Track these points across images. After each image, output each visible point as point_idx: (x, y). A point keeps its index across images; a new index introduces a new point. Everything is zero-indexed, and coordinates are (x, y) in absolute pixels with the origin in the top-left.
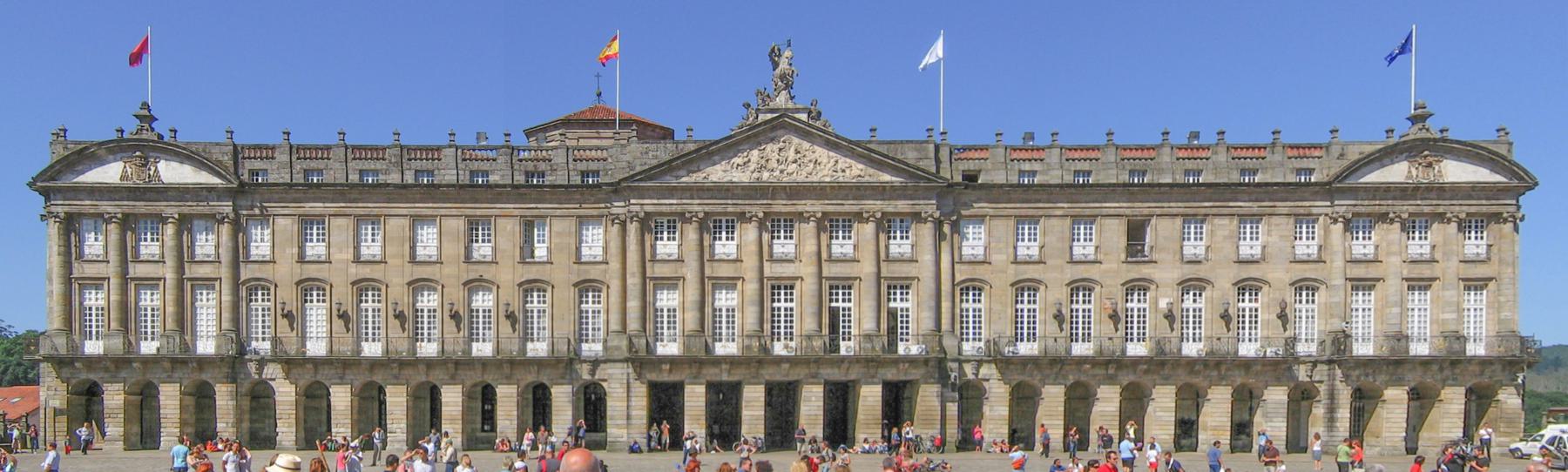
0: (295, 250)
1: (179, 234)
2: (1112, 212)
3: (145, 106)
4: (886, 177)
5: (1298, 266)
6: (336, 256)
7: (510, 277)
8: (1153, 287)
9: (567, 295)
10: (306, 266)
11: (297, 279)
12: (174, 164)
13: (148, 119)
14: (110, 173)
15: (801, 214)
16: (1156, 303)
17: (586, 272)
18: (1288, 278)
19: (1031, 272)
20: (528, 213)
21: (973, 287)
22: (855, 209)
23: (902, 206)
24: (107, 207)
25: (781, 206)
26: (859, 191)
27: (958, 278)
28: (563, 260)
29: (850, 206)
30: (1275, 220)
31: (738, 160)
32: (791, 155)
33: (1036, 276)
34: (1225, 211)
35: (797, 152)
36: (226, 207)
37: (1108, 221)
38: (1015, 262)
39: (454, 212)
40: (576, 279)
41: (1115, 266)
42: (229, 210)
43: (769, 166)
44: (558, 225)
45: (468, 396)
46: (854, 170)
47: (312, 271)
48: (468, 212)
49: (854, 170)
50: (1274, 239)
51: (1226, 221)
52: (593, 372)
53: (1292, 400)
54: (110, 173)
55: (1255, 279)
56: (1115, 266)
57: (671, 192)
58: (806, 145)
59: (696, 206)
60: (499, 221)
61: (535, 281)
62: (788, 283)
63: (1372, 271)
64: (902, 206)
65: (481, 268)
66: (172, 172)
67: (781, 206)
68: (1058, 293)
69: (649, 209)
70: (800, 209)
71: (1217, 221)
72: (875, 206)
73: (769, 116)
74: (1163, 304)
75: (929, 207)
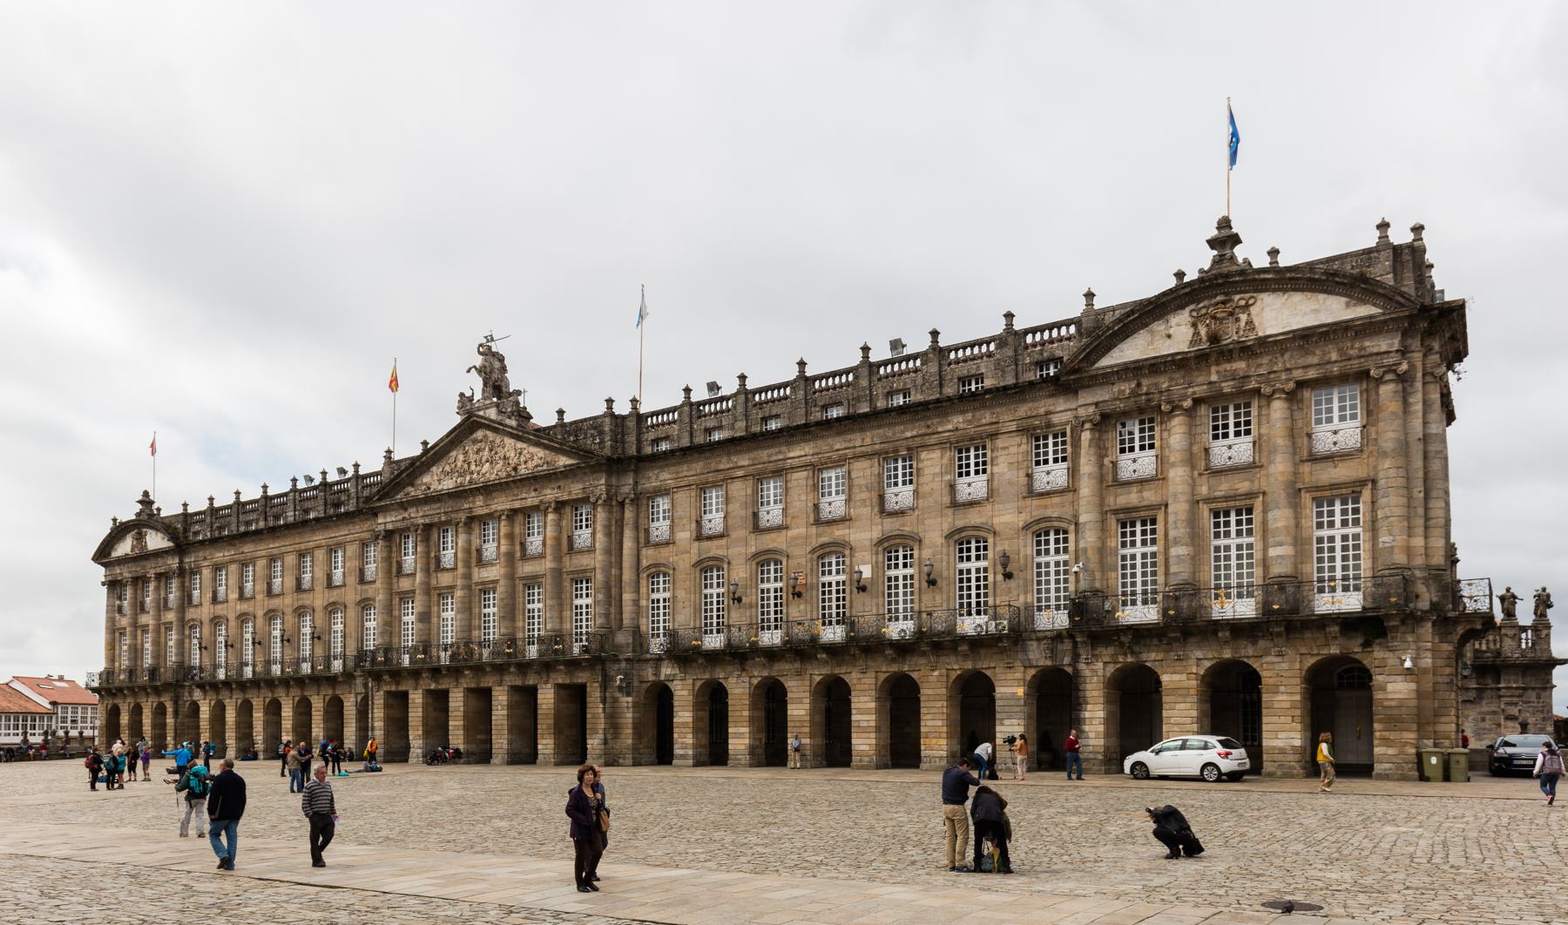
2: (796, 462)
4: (563, 461)
5: (1036, 502)
9: (352, 613)
14: (125, 548)
18: (1021, 521)
19: (715, 549)
20: (331, 542)
21: (656, 571)
22: (536, 501)
23: (575, 489)
24: (125, 573)
26: (536, 480)
27: (644, 563)
28: (352, 580)
29: (531, 499)
30: (1000, 442)
32: (486, 453)
33: (720, 553)
36: (174, 562)
37: (795, 476)
39: (290, 549)
41: (802, 530)
42: (176, 566)
46: (534, 458)
49: (534, 458)
54: (125, 548)
55: (975, 528)
56: (802, 530)
57: (403, 506)
59: (418, 516)
64: (575, 489)
68: (740, 572)
69: (390, 527)
70: (493, 507)
71: (924, 455)
72: (550, 494)
75: (600, 484)
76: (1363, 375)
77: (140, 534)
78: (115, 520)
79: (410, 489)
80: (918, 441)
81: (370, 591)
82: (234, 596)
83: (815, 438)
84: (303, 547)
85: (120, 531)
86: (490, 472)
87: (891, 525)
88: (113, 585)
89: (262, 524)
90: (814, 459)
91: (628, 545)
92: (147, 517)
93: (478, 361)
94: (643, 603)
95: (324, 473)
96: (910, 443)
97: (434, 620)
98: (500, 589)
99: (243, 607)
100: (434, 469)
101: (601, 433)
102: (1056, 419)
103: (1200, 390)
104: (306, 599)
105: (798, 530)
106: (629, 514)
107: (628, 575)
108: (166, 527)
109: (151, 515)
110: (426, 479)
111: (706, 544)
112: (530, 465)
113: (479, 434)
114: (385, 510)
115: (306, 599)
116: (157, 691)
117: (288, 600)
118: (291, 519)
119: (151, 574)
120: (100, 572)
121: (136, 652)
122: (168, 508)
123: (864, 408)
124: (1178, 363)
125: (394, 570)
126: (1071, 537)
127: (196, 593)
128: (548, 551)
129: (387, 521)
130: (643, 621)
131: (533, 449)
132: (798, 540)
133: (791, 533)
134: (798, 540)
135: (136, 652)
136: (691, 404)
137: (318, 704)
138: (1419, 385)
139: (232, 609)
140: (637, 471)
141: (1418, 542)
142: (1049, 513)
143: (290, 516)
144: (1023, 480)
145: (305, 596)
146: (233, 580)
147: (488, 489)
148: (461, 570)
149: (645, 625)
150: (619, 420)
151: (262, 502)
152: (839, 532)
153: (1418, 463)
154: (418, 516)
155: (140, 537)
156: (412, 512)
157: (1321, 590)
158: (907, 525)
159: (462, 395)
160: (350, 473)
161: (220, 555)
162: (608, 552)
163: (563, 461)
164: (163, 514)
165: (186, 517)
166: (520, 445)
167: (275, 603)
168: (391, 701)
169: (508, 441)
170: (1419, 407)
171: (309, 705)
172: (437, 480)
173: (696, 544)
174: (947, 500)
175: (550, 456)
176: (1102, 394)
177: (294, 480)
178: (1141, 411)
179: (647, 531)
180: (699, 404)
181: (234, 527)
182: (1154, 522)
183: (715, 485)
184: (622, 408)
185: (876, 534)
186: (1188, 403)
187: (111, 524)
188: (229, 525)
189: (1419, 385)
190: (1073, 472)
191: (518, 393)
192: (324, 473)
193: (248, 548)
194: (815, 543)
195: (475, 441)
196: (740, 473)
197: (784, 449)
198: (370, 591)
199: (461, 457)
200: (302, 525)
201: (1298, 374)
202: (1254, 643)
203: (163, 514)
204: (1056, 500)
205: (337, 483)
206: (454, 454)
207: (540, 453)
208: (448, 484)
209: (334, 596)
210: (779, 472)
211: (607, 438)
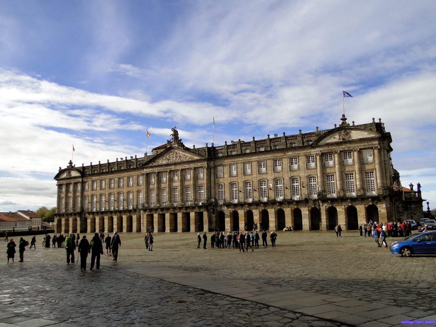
1: (74, 186)
2: (253, 160)
3: (71, 161)
4: (196, 158)
12: (73, 171)
13: (71, 163)
20: (129, 175)
23: (199, 165)
24: (64, 182)
25: (173, 168)
26: (188, 162)
31: (164, 158)
34: (285, 156)
36: (80, 180)
45: (100, 219)
51: (286, 160)
54: (64, 175)
57: (151, 167)
59: (156, 170)
63: (332, 171)
66: (74, 174)
67: (173, 168)
69: (148, 172)
70: (177, 169)
76: (372, 148)
77: (69, 172)
78: (60, 168)
80: (282, 157)
81: (140, 188)
82: (98, 189)
84: (120, 176)
85: (61, 172)
87: (277, 175)
88: (60, 186)
89: (107, 170)
90: (258, 160)
91: (212, 178)
92: (71, 167)
93: (172, 133)
94: (216, 192)
95: (126, 157)
96: (280, 157)
97: (160, 196)
98: (179, 188)
99: (102, 192)
101: (205, 151)
102: (312, 153)
103: (341, 149)
104: (121, 190)
105: (254, 175)
106: (212, 171)
107: (212, 185)
108: (78, 170)
109: (72, 167)
111: (232, 178)
114: (146, 168)
115: (121, 190)
116: (75, 214)
117: (115, 190)
118: (116, 169)
119: (73, 182)
120: (56, 182)
121: (67, 204)
122: (78, 164)
123: (269, 149)
124: (337, 144)
125: (148, 183)
126: (317, 179)
127: (87, 187)
128: (192, 179)
129: (146, 171)
130: (216, 196)
132: (255, 178)
134: (255, 178)
135: (67, 204)
136: (227, 145)
137: (125, 217)
138: (382, 150)
139: (98, 192)
140: (214, 161)
141: (385, 181)
142: (311, 173)
143: (116, 168)
144: (305, 166)
145: (121, 189)
146: (99, 184)
147: (175, 164)
148: (167, 184)
149: (217, 198)
150: (209, 148)
151: (108, 164)
152: (265, 176)
153: (384, 166)
154: (156, 170)
155: (69, 173)
156: (154, 169)
157: (368, 191)
158: (280, 175)
159: (168, 141)
160: (134, 158)
161: (94, 178)
162: (207, 180)
163: (196, 158)
164: (76, 166)
165: (84, 168)
166: (184, 153)
167: (111, 191)
168: (148, 216)
169: (181, 152)
170: (383, 155)
171: (122, 218)
173: (229, 178)
174: (289, 170)
176: (321, 149)
177: (117, 159)
178: (329, 153)
179: (217, 175)
180: (229, 146)
181: (99, 170)
182: (333, 176)
183: (234, 164)
184: (210, 146)
185: (273, 177)
186: (339, 152)
187: (59, 169)
188: (97, 170)
189: (382, 150)
190: (316, 164)
191: (181, 140)
192: (126, 157)
193: (103, 177)
194: (258, 179)
196: (240, 162)
198: (140, 188)
200: (119, 171)
201: (360, 147)
202: (355, 202)
203: (76, 166)
204: (313, 170)
205: (130, 160)
207: (189, 155)
208: (165, 162)
209: (129, 189)
210: (250, 162)
211: (207, 153)
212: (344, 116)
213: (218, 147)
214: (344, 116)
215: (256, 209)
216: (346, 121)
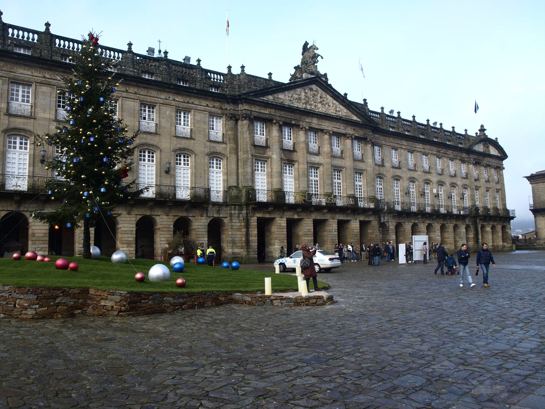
0: (4, 105)
4: (355, 118)
6: (40, 114)
7: (168, 145)
8: (431, 184)
10: (12, 119)
11: (5, 127)
15: (322, 130)
16: (432, 190)
17: (214, 147)
22: (344, 132)
23: (360, 133)
25: (315, 122)
35: (321, 97)
38: (393, 167)
39: (132, 96)
40: (207, 151)
41: (420, 173)
43: (310, 103)
44: (199, 116)
46: (343, 112)
47: (19, 123)
48: (142, 97)
49: (343, 112)
50: (457, 169)
52: (218, 212)
53: (502, 228)
57: (267, 105)
58: (324, 94)
60: (164, 108)
61: (185, 149)
62: (317, 166)
65: (149, 137)
70: (323, 127)
73: (310, 76)
74: (435, 191)
79: (271, 97)
83: (424, 144)
84: (149, 99)
86: (321, 109)
100: (286, 93)
110: (281, 96)
112: (340, 113)
113: (314, 87)
131: (341, 106)
133: (418, 173)
163: (355, 118)
166: (335, 102)
172: (284, 98)
173: (392, 169)
175: (349, 114)
195: (311, 89)
196: (404, 147)
197: (416, 144)
199: (303, 94)
206: (299, 90)
207: (345, 110)
208: (301, 106)
212: (482, 126)
213: (373, 112)
214: (482, 126)
215: (423, 222)
216: (485, 132)
